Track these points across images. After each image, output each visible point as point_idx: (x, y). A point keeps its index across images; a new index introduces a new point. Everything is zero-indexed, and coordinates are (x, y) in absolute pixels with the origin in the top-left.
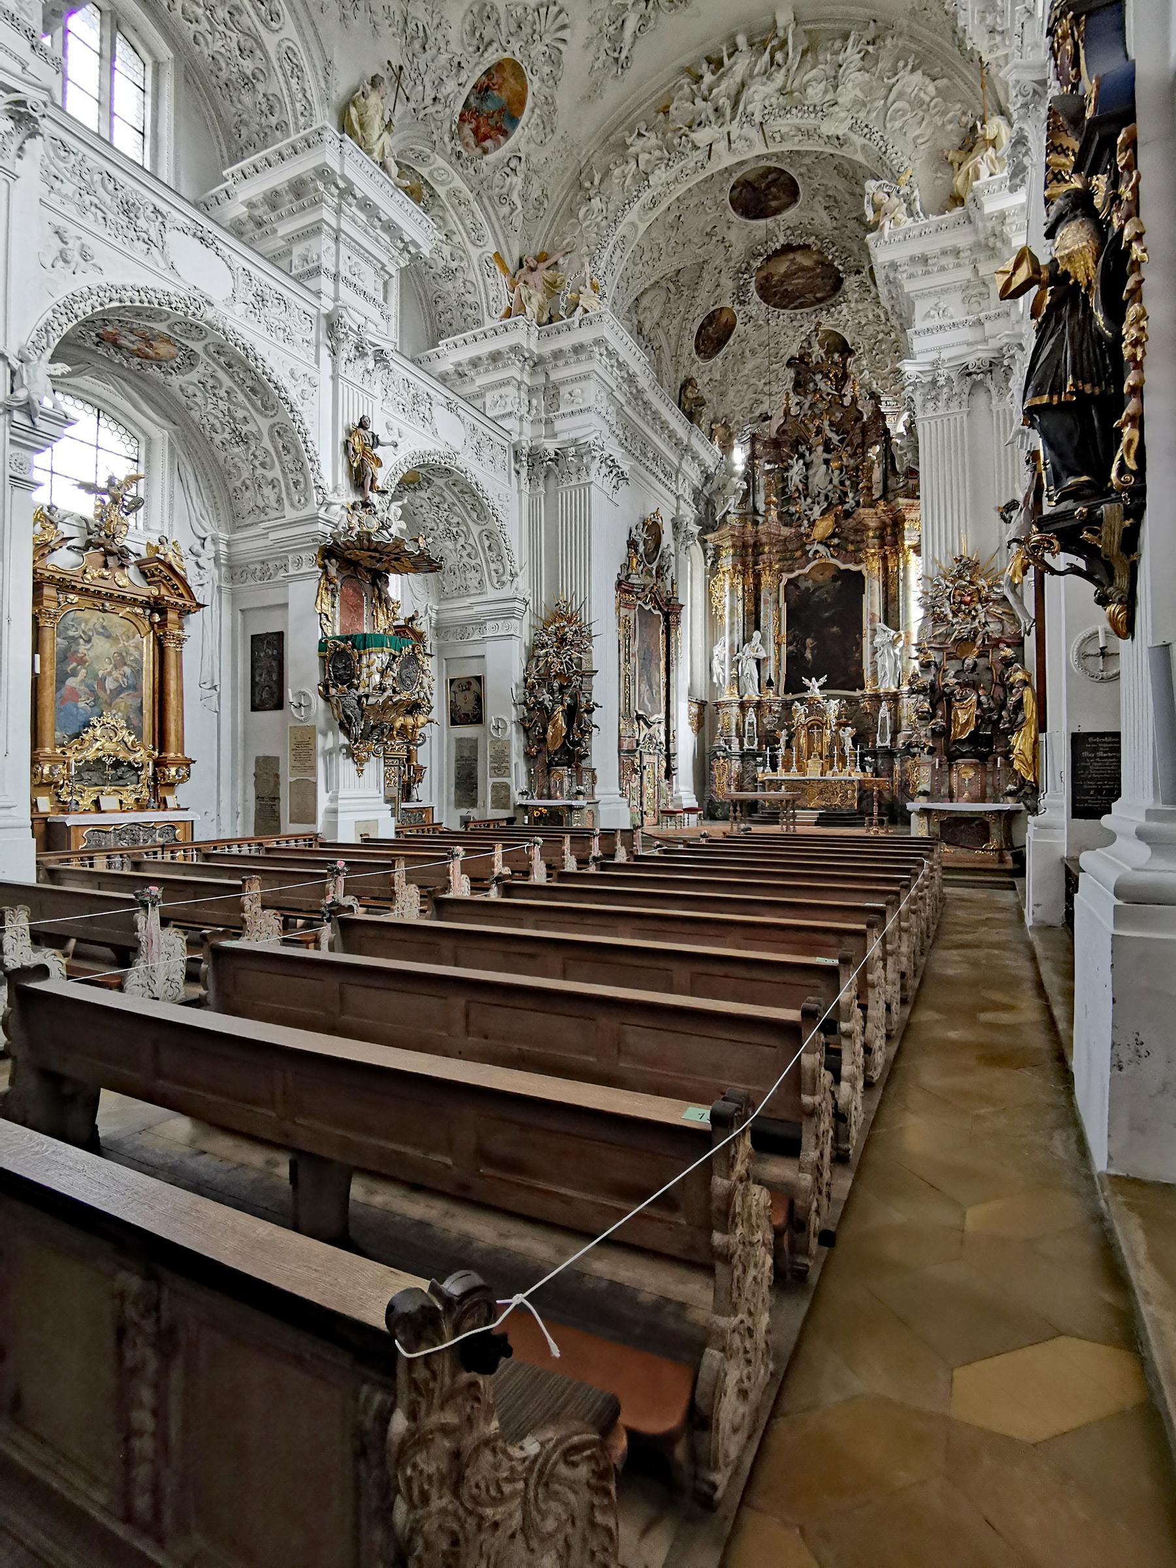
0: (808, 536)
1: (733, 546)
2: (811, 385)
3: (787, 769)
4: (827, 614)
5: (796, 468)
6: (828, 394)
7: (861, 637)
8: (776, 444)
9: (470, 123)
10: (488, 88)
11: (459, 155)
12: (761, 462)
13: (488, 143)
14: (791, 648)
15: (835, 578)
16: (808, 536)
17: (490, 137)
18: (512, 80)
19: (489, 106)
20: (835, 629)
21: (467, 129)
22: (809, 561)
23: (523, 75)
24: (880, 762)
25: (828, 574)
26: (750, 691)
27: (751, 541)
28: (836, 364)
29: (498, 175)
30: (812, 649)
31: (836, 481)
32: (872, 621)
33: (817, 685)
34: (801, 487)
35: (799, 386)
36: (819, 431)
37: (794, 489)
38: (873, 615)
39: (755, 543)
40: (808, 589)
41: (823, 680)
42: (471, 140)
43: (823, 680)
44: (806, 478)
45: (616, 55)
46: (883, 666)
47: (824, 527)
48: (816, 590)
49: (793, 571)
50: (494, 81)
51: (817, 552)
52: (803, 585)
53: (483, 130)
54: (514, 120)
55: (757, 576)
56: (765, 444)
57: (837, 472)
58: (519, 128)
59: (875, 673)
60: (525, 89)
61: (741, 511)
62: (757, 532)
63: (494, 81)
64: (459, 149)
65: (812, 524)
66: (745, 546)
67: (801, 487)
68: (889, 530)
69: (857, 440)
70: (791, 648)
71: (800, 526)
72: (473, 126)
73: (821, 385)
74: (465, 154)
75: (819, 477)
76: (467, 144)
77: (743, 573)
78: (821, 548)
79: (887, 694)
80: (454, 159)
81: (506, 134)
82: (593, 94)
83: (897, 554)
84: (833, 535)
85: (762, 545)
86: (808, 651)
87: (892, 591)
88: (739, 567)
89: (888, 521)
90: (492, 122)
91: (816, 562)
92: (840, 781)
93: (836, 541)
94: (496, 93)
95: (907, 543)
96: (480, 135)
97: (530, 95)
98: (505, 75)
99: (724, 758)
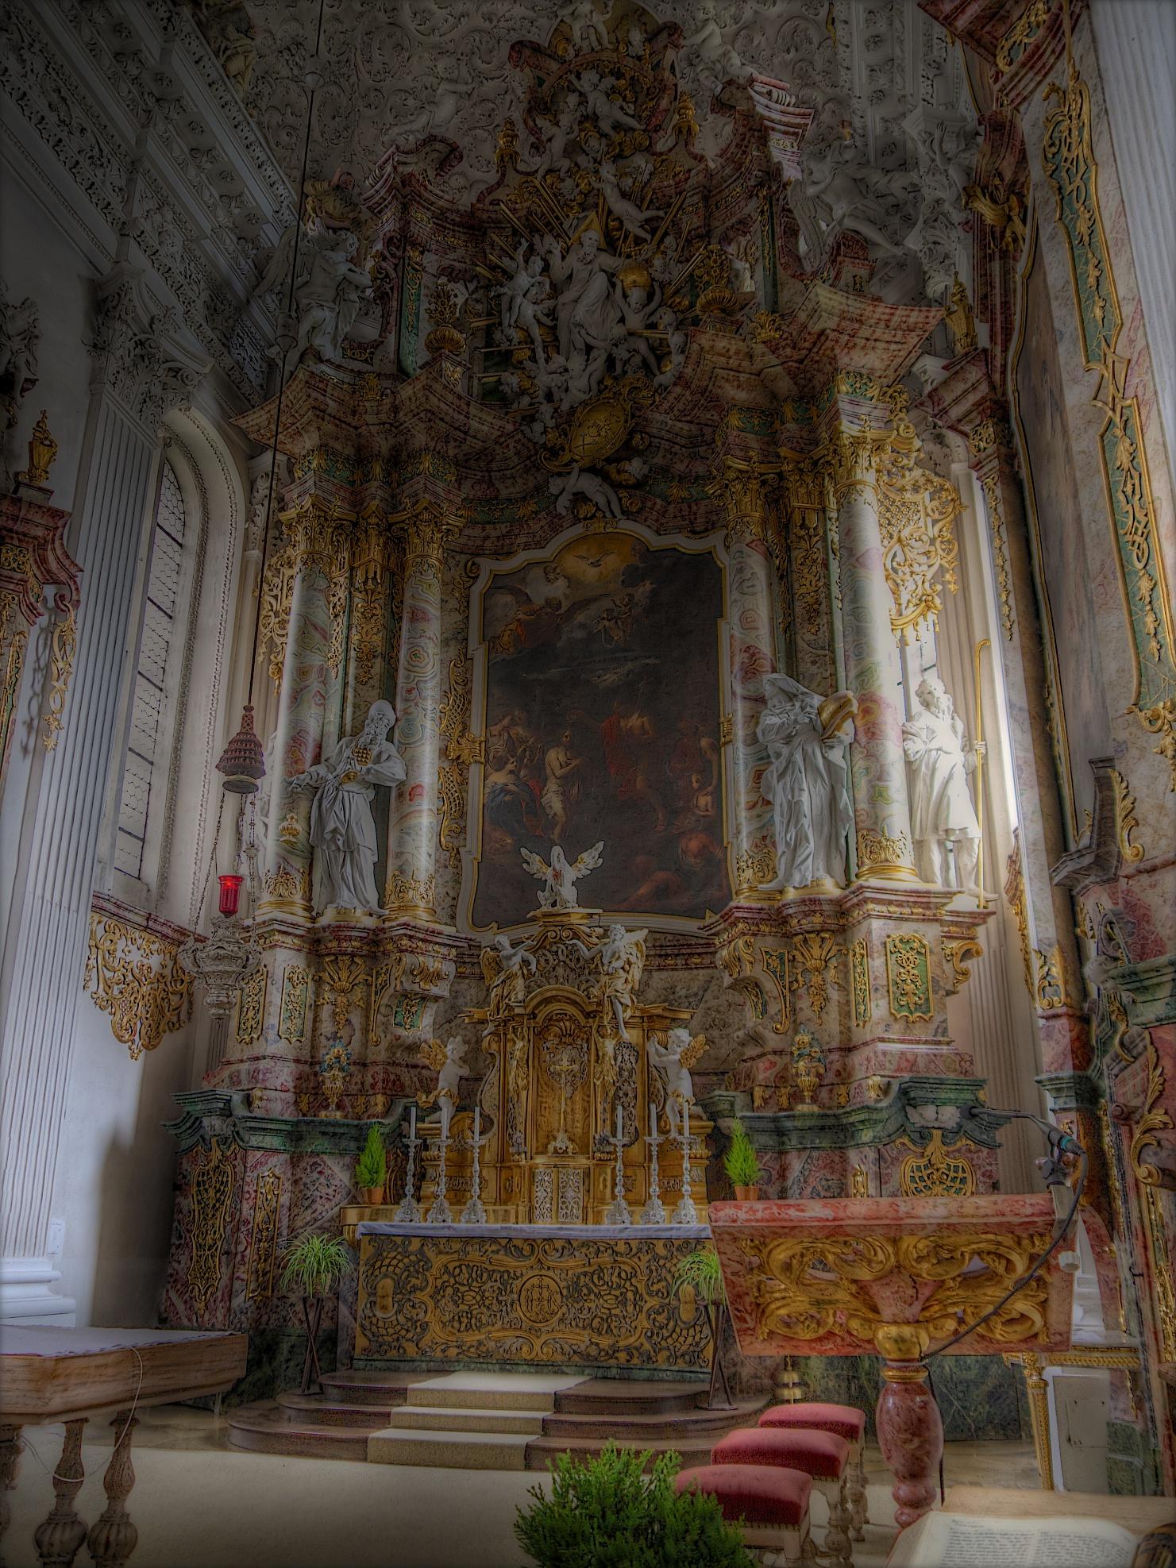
0: (554, 452)
1: (323, 448)
2: (573, 99)
3: (458, 1195)
4: (610, 678)
5: (523, 280)
6: (617, 127)
7: (717, 748)
8: (474, 226)
12: (431, 261)
14: (499, 778)
15: (632, 577)
16: (554, 452)
20: (635, 721)
22: (556, 530)
24: (796, 1164)
25: (613, 563)
26: (346, 897)
27: (383, 444)
28: (639, 58)
30: (565, 781)
31: (635, 321)
32: (751, 671)
33: (570, 874)
34: (536, 332)
35: (541, 105)
36: (590, 200)
37: (516, 335)
38: (751, 652)
39: (396, 451)
40: (552, 604)
41: (590, 859)
43: (590, 859)
44: (555, 319)
46: (794, 808)
47: (596, 434)
48: (577, 607)
49: (509, 554)
51: (580, 498)
52: (542, 591)
55: (397, 542)
56: (441, 219)
57: (636, 296)
59: (764, 840)
61: (357, 366)
62: (395, 409)
65: (567, 422)
66: (361, 459)
67: (536, 332)
68: (788, 411)
69: (691, 222)
70: (499, 778)
71: (530, 419)
73: (598, 102)
75: (585, 306)
77: (351, 531)
78: (589, 485)
79: (811, 904)
83: (818, 475)
84: (627, 451)
85: (415, 456)
86: (552, 786)
87: (806, 583)
88: (338, 508)
89: (784, 385)
91: (578, 530)
92: (648, 1243)
93: (635, 468)
95: (849, 429)
99: (224, 1141)
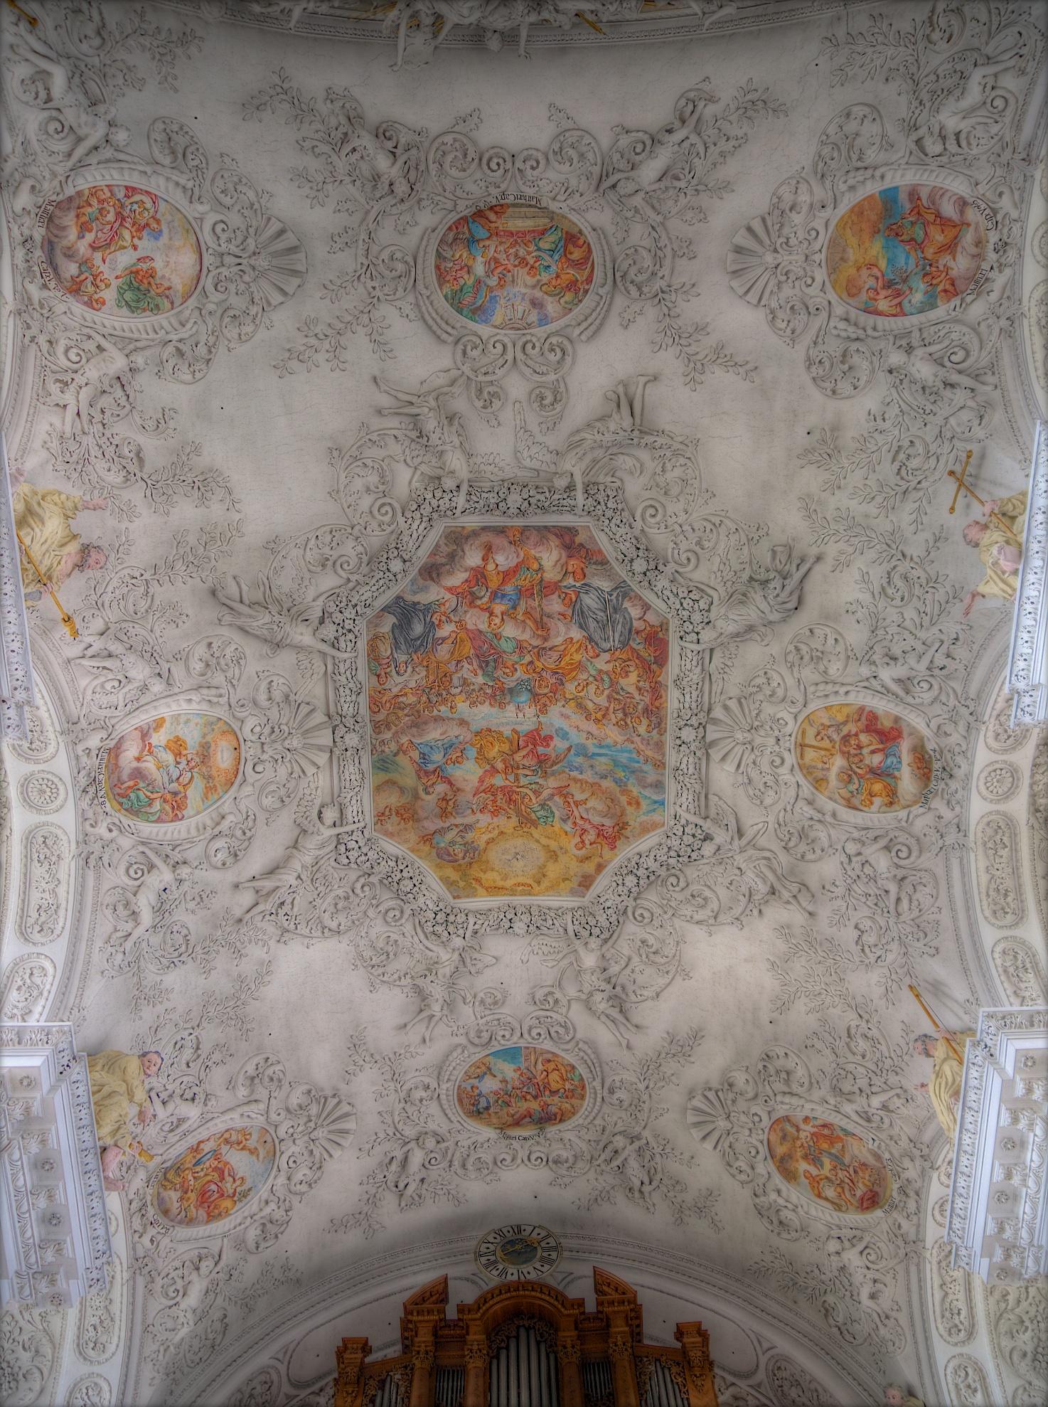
9: (947, 268)
10: (889, 285)
11: (1002, 247)
13: (948, 210)
17: (938, 215)
18: (851, 255)
19: (906, 259)
21: (960, 264)
23: (833, 243)
29: (975, 151)
42: (968, 238)
45: (694, 138)
50: (871, 282)
53: (939, 238)
54: (889, 199)
58: (888, 184)
60: (842, 224)
63: (871, 282)
64: (992, 256)
72: (945, 259)
74: (993, 237)
76: (978, 243)
80: (1012, 254)
81: (914, 194)
82: (758, 104)
90: (919, 233)
94: (883, 264)
96: (951, 233)
97: (843, 208)
98: (853, 271)
